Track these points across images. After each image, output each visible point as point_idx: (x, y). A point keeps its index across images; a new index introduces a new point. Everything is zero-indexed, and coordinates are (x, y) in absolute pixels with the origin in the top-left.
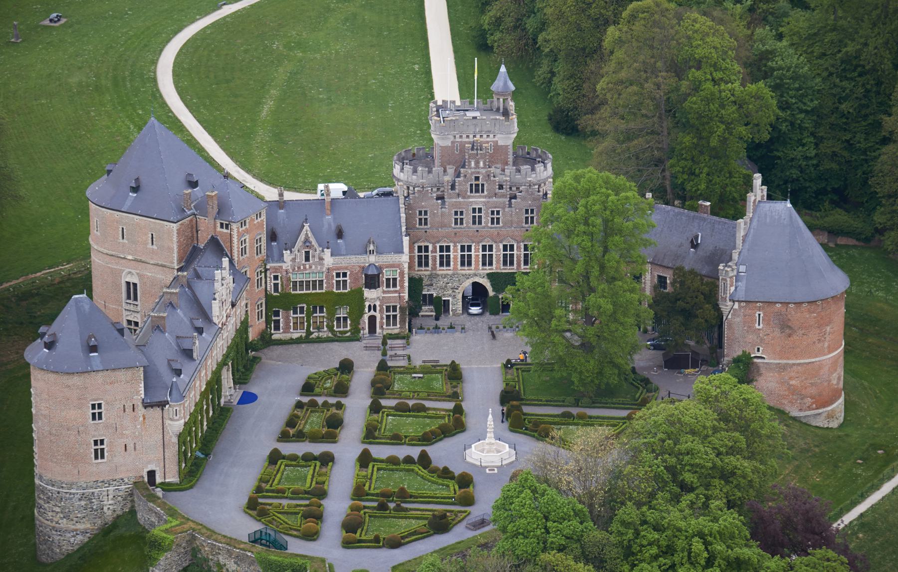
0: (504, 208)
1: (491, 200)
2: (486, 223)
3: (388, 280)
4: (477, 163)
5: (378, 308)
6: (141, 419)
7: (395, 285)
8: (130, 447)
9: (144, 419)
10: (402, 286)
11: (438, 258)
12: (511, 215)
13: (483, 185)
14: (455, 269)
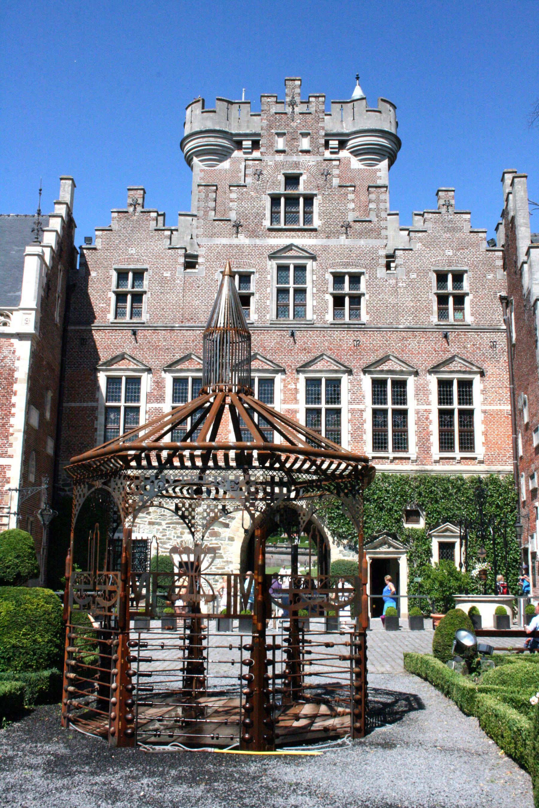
0: (372, 267)
1: (332, 242)
2: (320, 311)
12: (395, 288)
13: (309, 200)
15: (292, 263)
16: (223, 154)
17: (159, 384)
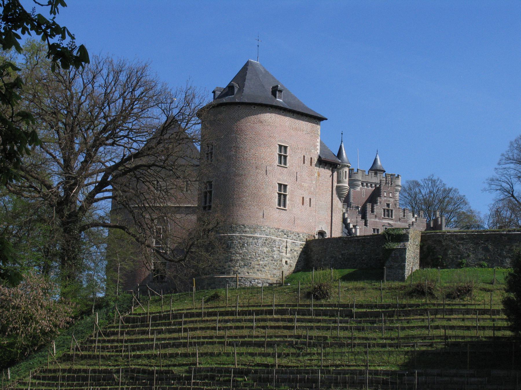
1: (397, 223)
6: (316, 175)
8: (307, 200)
9: (319, 175)
13: (392, 211)
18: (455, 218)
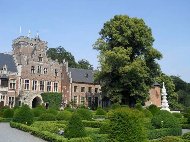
0: (48, 68)
2: (42, 73)
3: (11, 84)
4: (41, 49)
5: (5, 98)
7: (14, 87)
10: (17, 88)
11: (24, 85)
12: (51, 71)
13: (42, 58)
14: (30, 90)
15: (40, 66)
16: (26, 45)
17: (23, 80)
18: (135, 81)
